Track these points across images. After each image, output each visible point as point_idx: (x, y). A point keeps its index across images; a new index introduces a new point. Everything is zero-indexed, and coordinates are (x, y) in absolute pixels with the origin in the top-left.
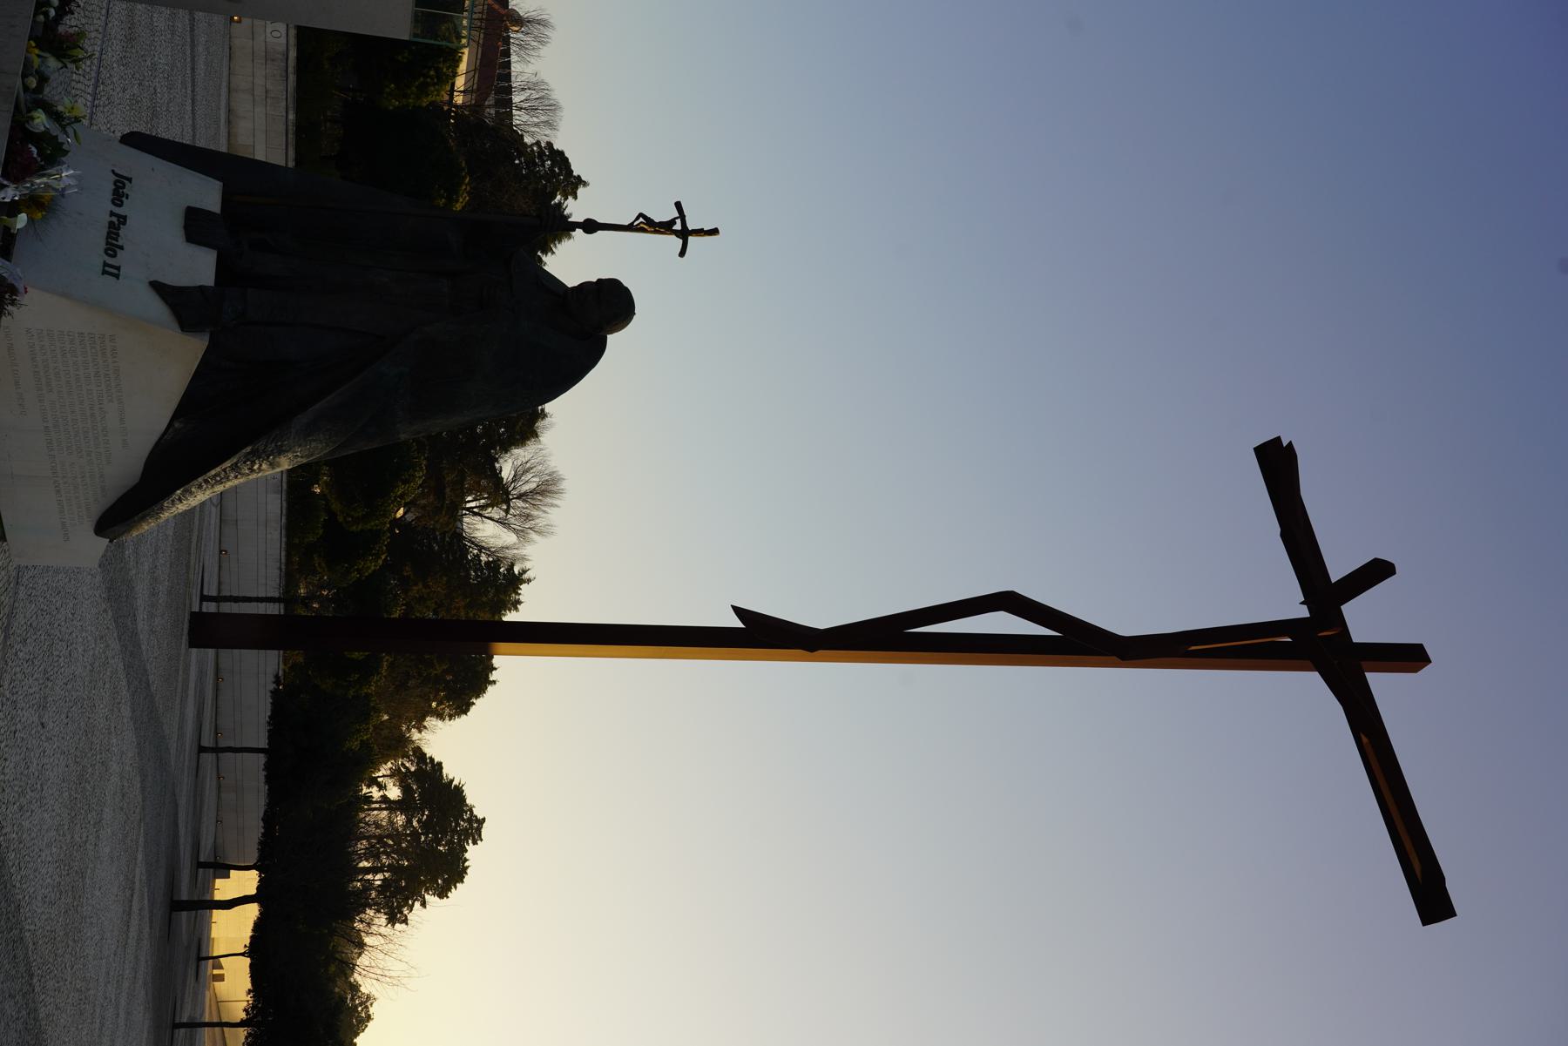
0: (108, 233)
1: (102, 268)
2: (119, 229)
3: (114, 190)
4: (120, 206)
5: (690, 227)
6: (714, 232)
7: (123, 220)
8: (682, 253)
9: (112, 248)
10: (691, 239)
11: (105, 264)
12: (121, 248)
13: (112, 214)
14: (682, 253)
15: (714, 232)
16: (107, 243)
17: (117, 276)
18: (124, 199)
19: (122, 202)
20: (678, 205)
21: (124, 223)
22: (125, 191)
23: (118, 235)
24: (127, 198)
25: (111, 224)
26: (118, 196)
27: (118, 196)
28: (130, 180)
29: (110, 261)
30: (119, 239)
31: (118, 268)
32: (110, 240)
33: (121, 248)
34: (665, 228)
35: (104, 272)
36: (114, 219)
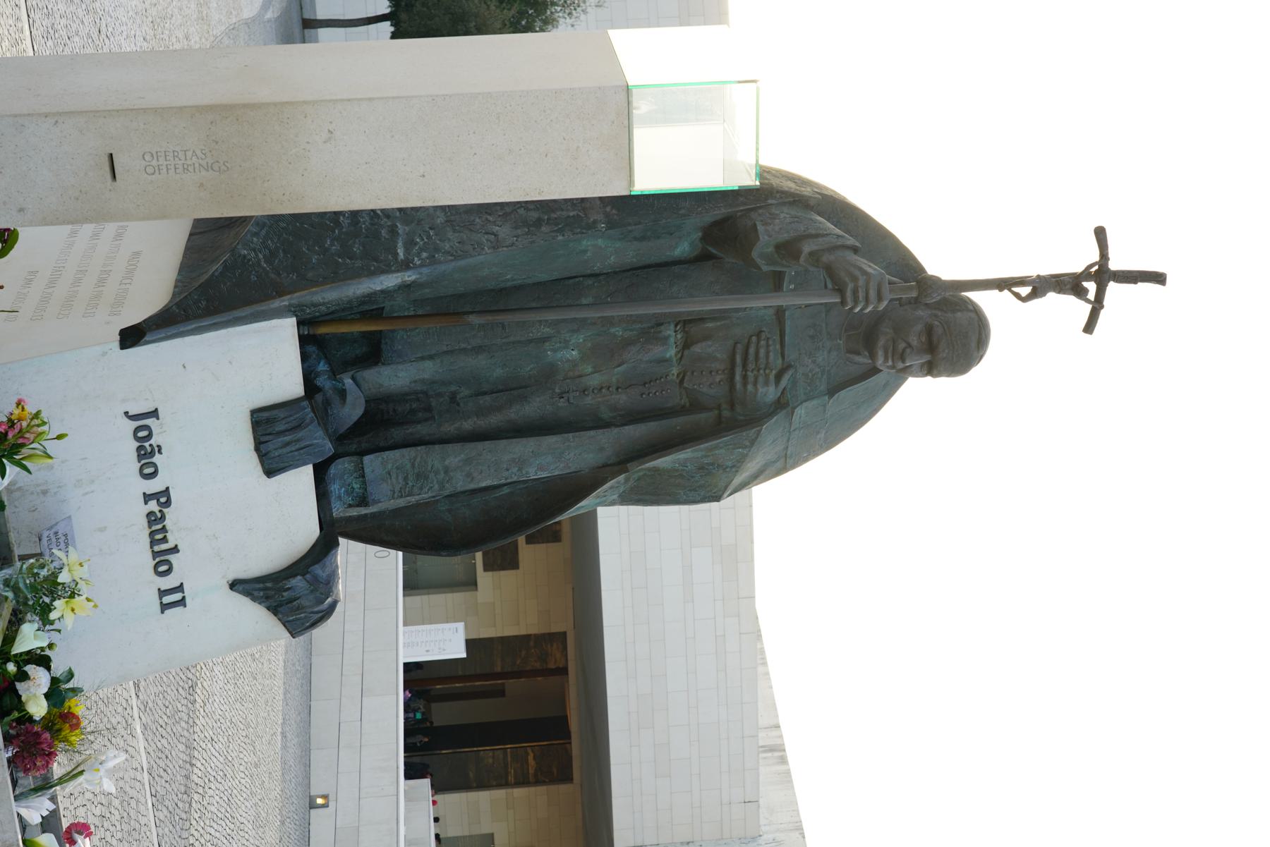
0: (152, 534)
1: (159, 602)
2: (163, 518)
3: (139, 449)
4: (154, 475)
5: (1114, 265)
6: (1158, 278)
7: (163, 498)
8: (1089, 327)
9: (163, 560)
10: (1112, 287)
11: (162, 593)
12: (175, 550)
13: (147, 498)
14: (1089, 327)
15: (1158, 278)
16: (155, 554)
17: (182, 602)
18: (157, 459)
19: (155, 465)
20: (1100, 234)
21: (168, 503)
22: (152, 442)
23: (164, 529)
24: (160, 452)
25: (154, 519)
26: (147, 455)
27: (147, 455)
28: (154, 414)
29: (167, 583)
30: (169, 536)
31: (180, 588)
32: (157, 548)
33: (175, 550)
34: (1070, 284)
35: (164, 607)
36: (153, 506)
